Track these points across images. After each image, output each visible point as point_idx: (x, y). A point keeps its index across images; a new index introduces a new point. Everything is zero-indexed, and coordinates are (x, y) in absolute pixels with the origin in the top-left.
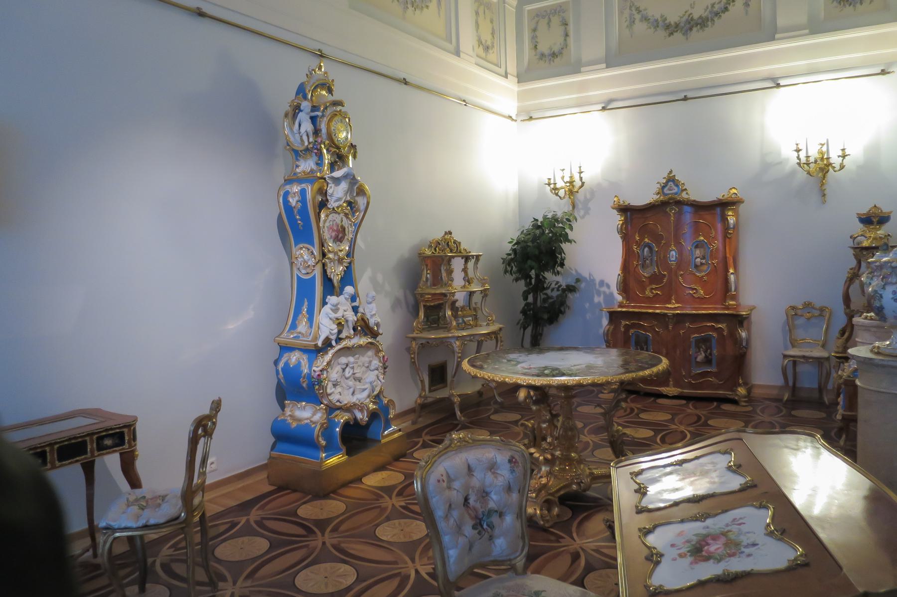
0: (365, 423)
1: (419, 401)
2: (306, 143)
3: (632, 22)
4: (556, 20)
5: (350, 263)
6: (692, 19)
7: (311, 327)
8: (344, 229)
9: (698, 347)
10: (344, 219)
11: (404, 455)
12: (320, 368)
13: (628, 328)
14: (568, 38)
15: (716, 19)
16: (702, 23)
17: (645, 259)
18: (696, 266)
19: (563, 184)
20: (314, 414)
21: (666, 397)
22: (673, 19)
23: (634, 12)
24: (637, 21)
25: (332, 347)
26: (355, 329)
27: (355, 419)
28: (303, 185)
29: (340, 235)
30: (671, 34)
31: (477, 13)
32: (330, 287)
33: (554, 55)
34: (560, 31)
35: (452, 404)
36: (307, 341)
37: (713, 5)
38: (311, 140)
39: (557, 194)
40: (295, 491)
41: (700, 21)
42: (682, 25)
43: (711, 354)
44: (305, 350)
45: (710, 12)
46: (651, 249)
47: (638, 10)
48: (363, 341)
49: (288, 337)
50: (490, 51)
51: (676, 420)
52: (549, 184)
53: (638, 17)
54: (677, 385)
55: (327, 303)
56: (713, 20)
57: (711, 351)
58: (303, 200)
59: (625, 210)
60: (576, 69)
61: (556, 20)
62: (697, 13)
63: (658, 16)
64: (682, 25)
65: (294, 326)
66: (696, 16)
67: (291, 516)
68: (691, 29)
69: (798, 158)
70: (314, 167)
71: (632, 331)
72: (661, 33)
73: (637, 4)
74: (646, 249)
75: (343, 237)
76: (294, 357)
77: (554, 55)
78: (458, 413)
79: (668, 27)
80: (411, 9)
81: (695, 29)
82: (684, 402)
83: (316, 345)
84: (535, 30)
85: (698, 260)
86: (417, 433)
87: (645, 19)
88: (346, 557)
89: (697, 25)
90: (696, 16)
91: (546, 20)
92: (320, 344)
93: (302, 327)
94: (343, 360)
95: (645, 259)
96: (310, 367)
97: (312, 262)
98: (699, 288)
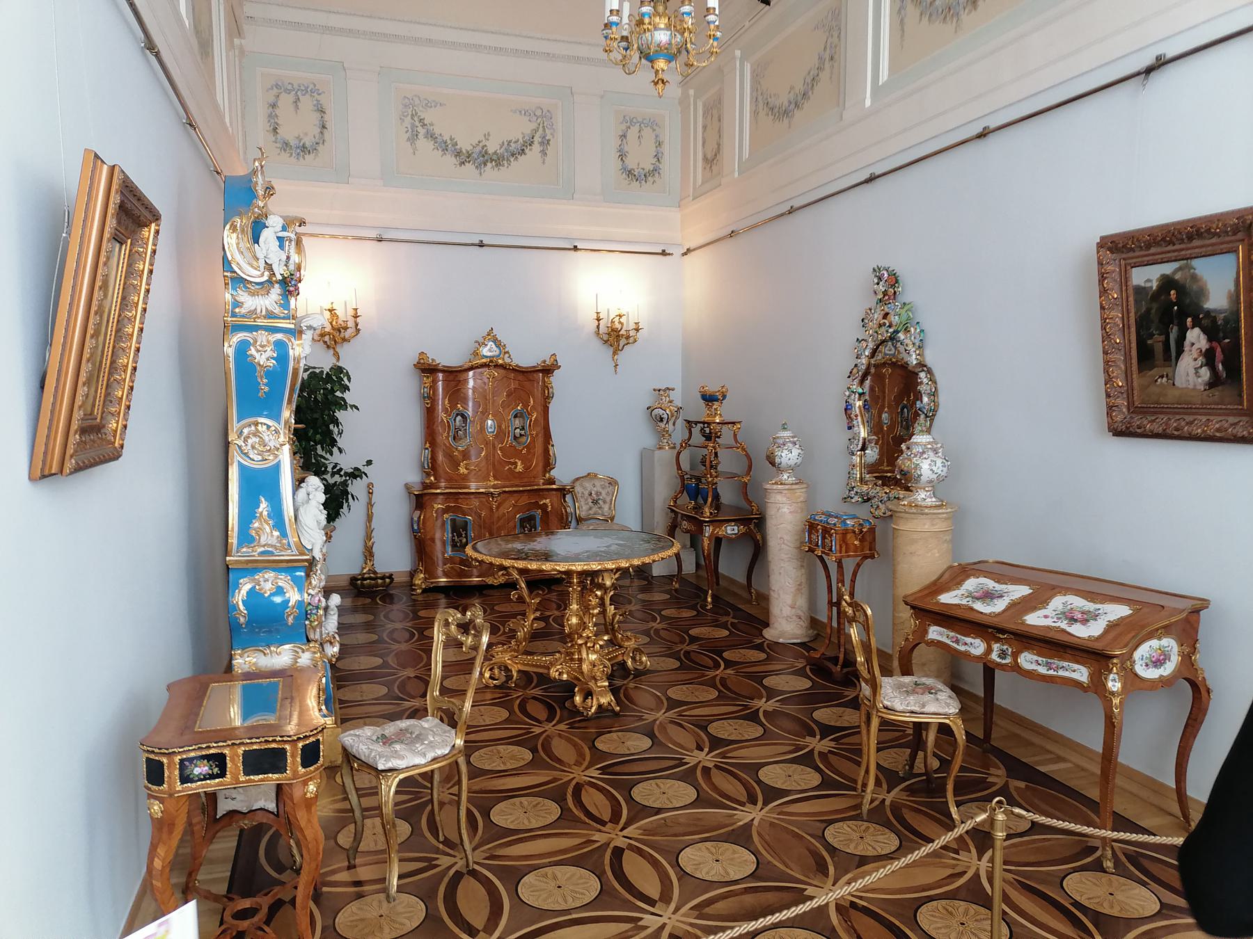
4: (307, 103)
7: (284, 534)
17: (457, 430)
18: (515, 438)
21: (492, 587)
22: (465, 145)
23: (417, 123)
33: (304, 149)
41: (495, 157)
44: (287, 567)
59: (427, 369)
60: (342, 174)
62: (492, 147)
63: (446, 138)
65: (246, 538)
69: (598, 327)
72: (450, 160)
74: (459, 418)
77: (304, 149)
79: (458, 154)
81: (489, 164)
84: (274, 106)
87: (431, 136)
89: (492, 160)
90: (491, 151)
91: (291, 98)
93: (268, 536)
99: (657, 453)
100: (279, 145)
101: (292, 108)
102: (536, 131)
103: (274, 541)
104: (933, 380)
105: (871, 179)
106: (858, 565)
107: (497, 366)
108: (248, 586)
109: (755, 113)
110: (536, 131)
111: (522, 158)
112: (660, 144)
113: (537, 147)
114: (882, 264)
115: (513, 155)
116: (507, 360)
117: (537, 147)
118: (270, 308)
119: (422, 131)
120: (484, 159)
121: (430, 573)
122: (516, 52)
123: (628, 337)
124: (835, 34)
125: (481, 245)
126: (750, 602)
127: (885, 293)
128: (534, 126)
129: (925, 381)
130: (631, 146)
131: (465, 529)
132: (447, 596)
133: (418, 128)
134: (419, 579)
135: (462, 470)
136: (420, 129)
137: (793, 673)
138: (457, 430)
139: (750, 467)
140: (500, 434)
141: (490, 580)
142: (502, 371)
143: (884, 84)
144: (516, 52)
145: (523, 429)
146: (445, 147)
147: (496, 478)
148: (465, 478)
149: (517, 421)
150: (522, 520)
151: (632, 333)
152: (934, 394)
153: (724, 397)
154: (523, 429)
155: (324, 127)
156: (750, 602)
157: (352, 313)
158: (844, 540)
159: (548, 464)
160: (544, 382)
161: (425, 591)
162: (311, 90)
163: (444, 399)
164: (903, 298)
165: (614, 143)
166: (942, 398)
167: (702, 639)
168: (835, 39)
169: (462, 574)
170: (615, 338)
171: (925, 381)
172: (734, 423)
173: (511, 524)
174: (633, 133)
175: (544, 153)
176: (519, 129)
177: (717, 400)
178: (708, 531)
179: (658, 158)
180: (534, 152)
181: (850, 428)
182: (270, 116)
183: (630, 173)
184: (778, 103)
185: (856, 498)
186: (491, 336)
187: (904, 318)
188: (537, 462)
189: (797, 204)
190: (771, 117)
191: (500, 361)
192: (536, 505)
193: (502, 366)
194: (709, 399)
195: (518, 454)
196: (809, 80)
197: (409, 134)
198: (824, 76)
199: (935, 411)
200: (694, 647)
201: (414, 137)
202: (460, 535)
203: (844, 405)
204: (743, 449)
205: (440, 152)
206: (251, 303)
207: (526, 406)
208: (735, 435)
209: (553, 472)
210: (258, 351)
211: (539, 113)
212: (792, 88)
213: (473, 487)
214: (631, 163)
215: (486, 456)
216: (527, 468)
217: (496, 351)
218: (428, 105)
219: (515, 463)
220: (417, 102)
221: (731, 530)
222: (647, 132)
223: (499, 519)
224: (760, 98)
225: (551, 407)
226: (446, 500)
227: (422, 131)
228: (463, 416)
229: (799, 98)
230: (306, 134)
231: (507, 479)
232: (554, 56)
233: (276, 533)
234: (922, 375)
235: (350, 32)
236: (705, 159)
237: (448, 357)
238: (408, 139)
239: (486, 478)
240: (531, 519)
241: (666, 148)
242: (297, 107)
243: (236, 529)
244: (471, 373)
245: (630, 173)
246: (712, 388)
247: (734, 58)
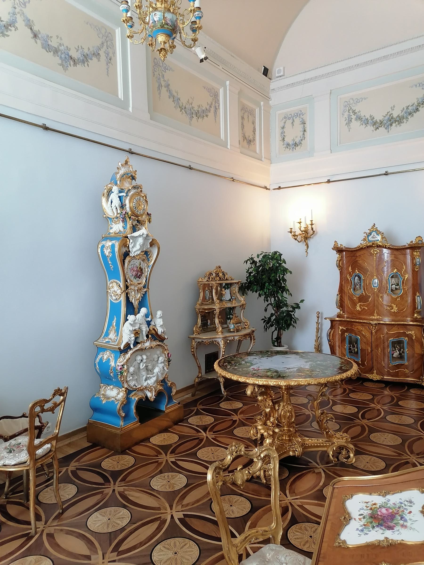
0: (152, 400)
1: (197, 381)
2: (116, 214)
3: (350, 120)
4: (297, 121)
5: (146, 292)
6: (392, 118)
7: (118, 335)
8: (141, 270)
9: (394, 347)
10: (142, 262)
11: (181, 421)
12: (122, 364)
13: (343, 332)
14: (305, 133)
15: (409, 117)
16: (400, 120)
17: (355, 285)
18: (392, 290)
19: (301, 232)
20: (118, 394)
21: (371, 381)
22: (378, 117)
23: (351, 114)
24: (353, 120)
25: (131, 349)
26: (147, 336)
27: (147, 397)
28: (114, 242)
29: (139, 274)
31: (243, 118)
32: (131, 309)
33: (296, 145)
34: (301, 127)
35: (219, 382)
36: (114, 345)
37: (407, 108)
38: (119, 212)
39: (296, 239)
40: (103, 447)
41: (398, 119)
43: (403, 352)
44: (113, 350)
45: (406, 113)
46: (360, 278)
47: (354, 112)
48: (154, 343)
49: (102, 341)
50: (252, 143)
51: (375, 400)
52: (291, 232)
53: (354, 117)
54: (379, 373)
55: (128, 320)
57: (404, 349)
58: (113, 252)
61: (297, 121)
63: (368, 116)
64: (385, 122)
65: (107, 334)
66: (395, 116)
67: (95, 468)
68: (391, 125)
70: (122, 229)
71: (346, 334)
72: (370, 128)
74: (357, 278)
75: (141, 275)
76: (106, 355)
78: (223, 389)
79: (375, 123)
80: (195, 118)
81: (394, 125)
82: (384, 385)
83: (120, 348)
84: (283, 128)
85: (394, 286)
86: (194, 403)
87: (359, 118)
88: (126, 502)
89: (396, 121)
90: (395, 116)
91: (291, 121)
92: (122, 348)
93: (112, 335)
94: (139, 358)
95: (355, 285)
96: (115, 362)
97: (119, 292)
100: (285, 146)
101: (291, 125)
115: (410, 114)
119: (354, 117)
120: (391, 121)
125: (386, 174)
131: (356, 343)
133: (352, 115)
145: (398, 285)
146: (366, 122)
147: (378, 314)
149: (393, 280)
150: (393, 343)
154: (398, 285)
155: (305, 131)
157: (310, 223)
162: (300, 114)
182: (282, 133)
186: (374, 229)
192: (404, 335)
202: (354, 347)
205: (364, 126)
218: (358, 101)
220: (351, 101)
230: (297, 137)
235: (316, 78)
238: (346, 124)
240: (400, 343)
242: (293, 125)
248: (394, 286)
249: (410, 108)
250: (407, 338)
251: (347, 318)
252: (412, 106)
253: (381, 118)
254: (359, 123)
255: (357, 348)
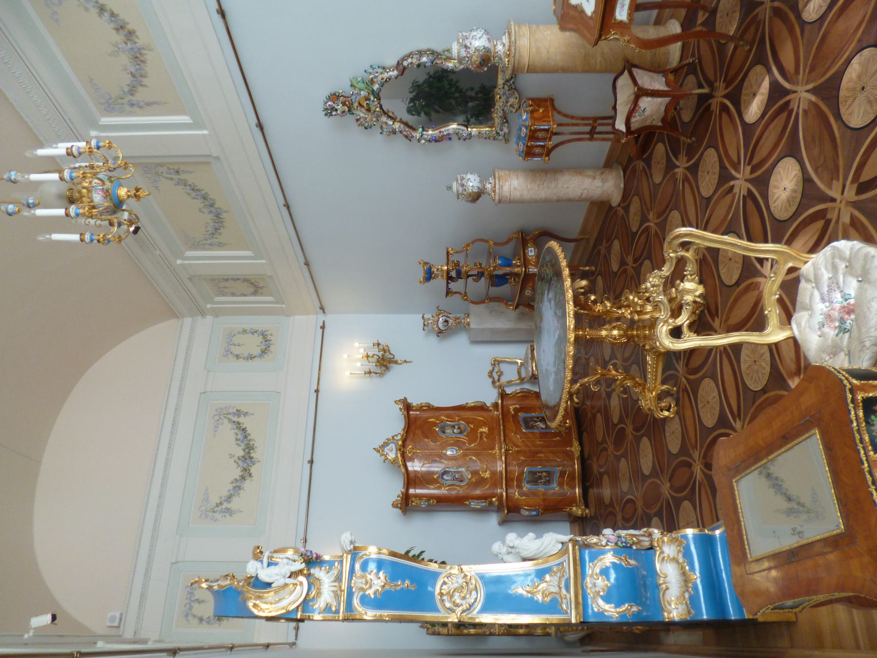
3: (229, 511)
6: (243, 457)
9: (532, 427)
16: (249, 448)
17: (454, 479)
21: (582, 452)
22: (237, 473)
23: (219, 508)
24: (229, 506)
30: (250, 475)
37: (237, 440)
41: (247, 451)
42: (245, 465)
43: (538, 418)
47: (217, 505)
56: (250, 440)
59: (406, 504)
63: (231, 487)
66: (242, 453)
68: (252, 458)
69: (376, 373)
72: (247, 484)
73: (214, 504)
74: (445, 477)
79: (243, 478)
81: (252, 455)
84: (201, 620)
85: (455, 431)
87: (229, 498)
89: (249, 453)
90: (242, 453)
91: (196, 606)
98: (481, 430)
99: (472, 326)
102: (230, 420)
103: (555, 580)
104: (410, 55)
105: (260, 126)
106: (559, 113)
107: (404, 445)
108: (601, 602)
109: (221, 246)
110: (230, 420)
111: (249, 431)
112: (245, 331)
113: (242, 419)
114: (321, 106)
115: (246, 437)
116: (399, 437)
117: (242, 419)
118: (332, 579)
119: (225, 505)
120: (247, 459)
121: (572, 501)
122: (173, 433)
123: (384, 350)
124: (161, 169)
125: (311, 462)
126: (588, 240)
127: (344, 104)
128: (226, 421)
129: (410, 60)
130: (244, 351)
131: (535, 473)
132: (591, 486)
133: (223, 508)
134: (577, 511)
135: (487, 475)
136: (224, 506)
137: (650, 167)
138: (454, 479)
139: (482, 240)
140: (457, 444)
141: (577, 454)
142: (408, 443)
143: (192, 118)
144: (173, 433)
145: (453, 427)
147: (493, 448)
148: (493, 473)
149: (448, 431)
150: (527, 427)
151: (381, 347)
152: (421, 53)
153: (426, 263)
156: (588, 240)
158: (539, 119)
159: (481, 408)
160: (416, 410)
161: (587, 506)
163: (429, 489)
164: (349, 91)
165: (241, 362)
166: (423, 46)
167: (622, 257)
168: (164, 169)
169: (572, 477)
170: (384, 361)
171: (410, 60)
172: (448, 253)
173: (530, 436)
174: (236, 350)
175: (246, 414)
176: (228, 432)
177: (430, 268)
178: (533, 270)
179: (253, 332)
180: (245, 421)
181: (450, 139)
182: (208, 623)
183: (264, 352)
184: (212, 224)
185: (506, 130)
186: (380, 450)
187: (362, 85)
188: (480, 417)
189: (283, 202)
190: (222, 230)
191: (400, 443)
192: (515, 416)
193: (404, 441)
194: (429, 276)
195: (474, 431)
196: (194, 194)
197: (227, 515)
198: (190, 178)
199: (433, 52)
200: (630, 259)
201: (229, 511)
202: (540, 478)
203: (433, 143)
204: (468, 245)
205: (242, 491)
206: (326, 596)
207: (435, 425)
208: (457, 252)
209: (488, 404)
210: (371, 587)
211: (217, 418)
212: (200, 211)
213: (500, 467)
214: (256, 351)
215: (475, 455)
216: (484, 424)
217: (392, 446)
219: (482, 433)
221: (531, 252)
222: (236, 340)
223: (526, 446)
224: (209, 241)
225: (436, 405)
226: (512, 487)
227: (225, 505)
228: (445, 473)
229: (207, 203)
231: (494, 439)
232: (177, 405)
233: (548, 577)
234: (405, 63)
236: (255, 293)
237: (395, 488)
238: (231, 515)
239: (493, 456)
240: (526, 421)
241: (248, 327)
242: (203, 601)
243: (544, 616)
244: (410, 469)
245: (264, 352)
246: (421, 275)
247: (182, 265)
248: (455, 431)
249: (239, 437)
250: (519, 414)
251: (502, 488)
252: (237, 434)
253: (239, 469)
254: (235, 500)
255: (542, 472)
